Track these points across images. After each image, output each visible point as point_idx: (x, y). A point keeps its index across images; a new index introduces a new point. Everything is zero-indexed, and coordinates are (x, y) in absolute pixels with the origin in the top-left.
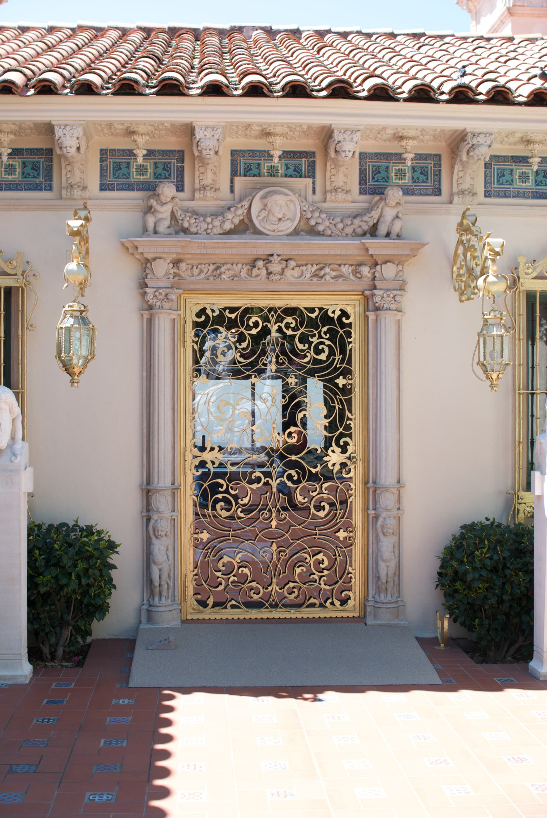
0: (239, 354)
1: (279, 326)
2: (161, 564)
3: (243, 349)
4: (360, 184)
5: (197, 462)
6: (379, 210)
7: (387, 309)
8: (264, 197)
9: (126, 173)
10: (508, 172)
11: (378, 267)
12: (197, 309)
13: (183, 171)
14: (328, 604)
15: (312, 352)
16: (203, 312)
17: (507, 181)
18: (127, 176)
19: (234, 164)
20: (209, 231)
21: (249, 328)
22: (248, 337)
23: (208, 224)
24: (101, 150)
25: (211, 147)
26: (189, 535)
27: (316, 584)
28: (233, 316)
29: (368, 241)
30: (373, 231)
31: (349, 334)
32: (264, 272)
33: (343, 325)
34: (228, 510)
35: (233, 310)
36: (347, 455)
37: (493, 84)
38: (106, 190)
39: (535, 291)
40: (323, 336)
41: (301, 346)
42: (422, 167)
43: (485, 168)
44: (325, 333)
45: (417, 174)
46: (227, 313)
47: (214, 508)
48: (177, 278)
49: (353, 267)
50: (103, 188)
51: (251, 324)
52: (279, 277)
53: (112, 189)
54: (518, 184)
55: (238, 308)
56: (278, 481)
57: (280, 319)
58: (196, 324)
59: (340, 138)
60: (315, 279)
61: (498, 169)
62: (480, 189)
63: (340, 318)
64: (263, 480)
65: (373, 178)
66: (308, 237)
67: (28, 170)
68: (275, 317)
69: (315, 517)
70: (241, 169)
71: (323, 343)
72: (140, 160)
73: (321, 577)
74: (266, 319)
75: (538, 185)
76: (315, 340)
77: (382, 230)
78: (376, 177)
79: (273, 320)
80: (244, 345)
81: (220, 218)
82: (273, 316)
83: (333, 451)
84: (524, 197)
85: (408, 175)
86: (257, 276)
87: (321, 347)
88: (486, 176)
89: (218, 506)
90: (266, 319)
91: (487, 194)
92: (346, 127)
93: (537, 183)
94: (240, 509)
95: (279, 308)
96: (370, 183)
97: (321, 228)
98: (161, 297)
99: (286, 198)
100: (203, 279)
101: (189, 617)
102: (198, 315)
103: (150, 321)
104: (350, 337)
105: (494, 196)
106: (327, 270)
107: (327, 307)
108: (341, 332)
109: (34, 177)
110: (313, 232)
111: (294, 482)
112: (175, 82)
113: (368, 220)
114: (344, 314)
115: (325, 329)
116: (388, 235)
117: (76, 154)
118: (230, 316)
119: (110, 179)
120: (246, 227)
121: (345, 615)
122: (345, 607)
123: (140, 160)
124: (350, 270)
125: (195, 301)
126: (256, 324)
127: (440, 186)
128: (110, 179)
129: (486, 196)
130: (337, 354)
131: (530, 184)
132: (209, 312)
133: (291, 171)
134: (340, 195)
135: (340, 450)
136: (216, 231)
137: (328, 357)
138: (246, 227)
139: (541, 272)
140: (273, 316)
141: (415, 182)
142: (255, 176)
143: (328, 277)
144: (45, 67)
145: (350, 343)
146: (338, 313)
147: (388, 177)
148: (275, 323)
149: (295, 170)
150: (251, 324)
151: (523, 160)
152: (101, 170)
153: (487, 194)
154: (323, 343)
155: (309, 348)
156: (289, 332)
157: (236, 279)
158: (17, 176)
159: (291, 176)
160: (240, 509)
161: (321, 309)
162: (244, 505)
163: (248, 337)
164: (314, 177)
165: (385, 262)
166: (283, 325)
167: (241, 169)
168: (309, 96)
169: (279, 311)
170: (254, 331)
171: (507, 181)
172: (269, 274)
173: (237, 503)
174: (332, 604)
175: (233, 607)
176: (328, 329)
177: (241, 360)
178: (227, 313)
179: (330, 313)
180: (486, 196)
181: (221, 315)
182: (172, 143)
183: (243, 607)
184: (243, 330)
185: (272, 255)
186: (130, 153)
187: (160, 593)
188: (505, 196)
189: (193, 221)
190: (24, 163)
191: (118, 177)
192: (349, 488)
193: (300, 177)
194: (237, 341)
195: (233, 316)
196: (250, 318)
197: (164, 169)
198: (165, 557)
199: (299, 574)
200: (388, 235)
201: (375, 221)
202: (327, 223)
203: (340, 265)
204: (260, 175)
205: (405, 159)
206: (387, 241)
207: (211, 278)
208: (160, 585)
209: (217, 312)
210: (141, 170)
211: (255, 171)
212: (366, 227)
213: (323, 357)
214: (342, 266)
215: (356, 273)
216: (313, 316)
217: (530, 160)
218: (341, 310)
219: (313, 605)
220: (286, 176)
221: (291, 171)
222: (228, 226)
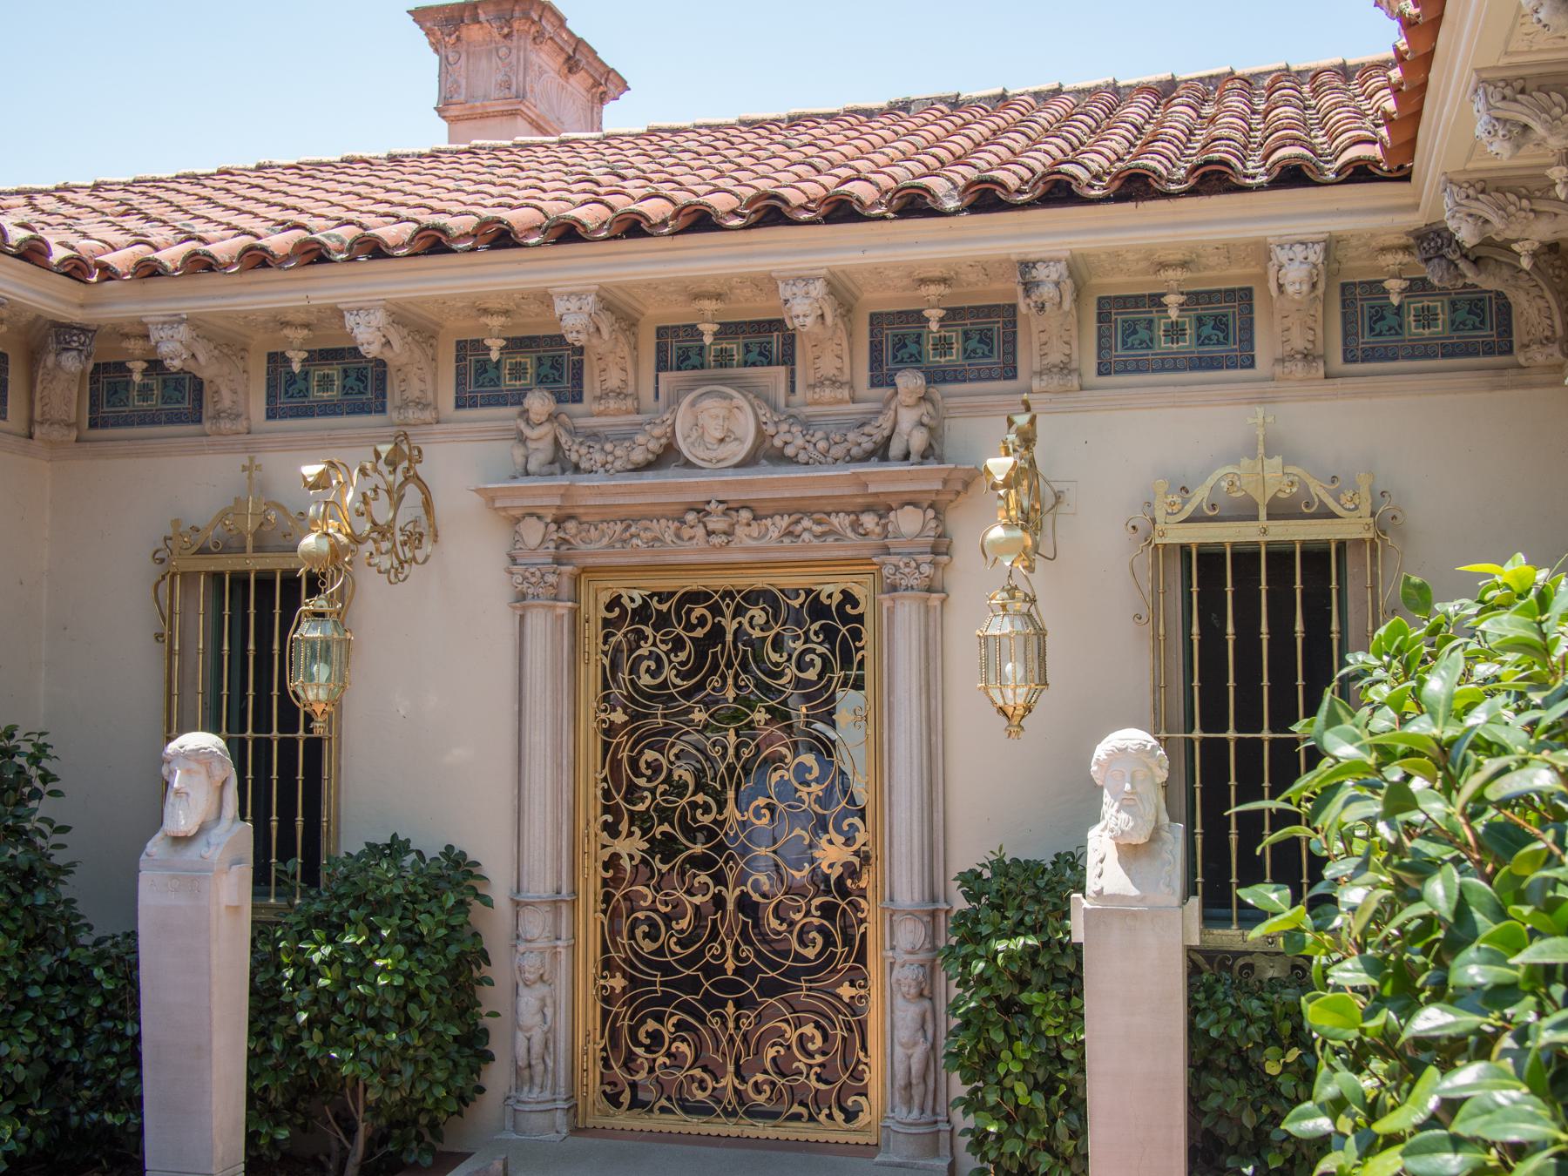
0: (674, 672)
1: (740, 623)
2: (530, 1029)
3: (682, 664)
4: (871, 370)
5: (605, 855)
6: (892, 413)
7: (906, 589)
8: (693, 404)
9: (1147, 338)
10: (1144, 324)
11: (892, 514)
12: (605, 598)
13: (581, 368)
14: (822, 1117)
15: (793, 667)
16: (615, 602)
17: (1142, 342)
18: (1149, 344)
19: (661, 350)
20: (608, 466)
21: (690, 627)
22: (689, 643)
23: (607, 454)
24: (458, 343)
25: (579, 327)
26: (873, 992)
27: (802, 1079)
28: (664, 607)
29: (873, 468)
30: (881, 452)
31: (857, 635)
32: (700, 531)
33: (846, 619)
34: (655, 939)
35: (663, 597)
36: (855, 847)
37: (307, 234)
38: (464, 406)
39: (1328, 542)
40: (814, 638)
41: (775, 657)
42: (1471, 301)
43: (1099, 321)
44: (816, 633)
45: (973, 344)
46: (654, 603)
47: (632, 936)
48: (564, 548)
49: (853, 517)
50: (271, 414)
51: (694, 621)
52: (724, 539)
53: (474, 405)
54: (1164, 345)
55: (673, 594)
56: (737, 892)
57: (739, 611)
58: (606, 623)
59: (788, 295)
60: (787, 540)
61: (1124, 321)
62: (1090, 363)
63: (840, 606)
64: (713, 890)
65: (895, 357)
66: (770, 467)
67: (351, 382)
68: (732, 607)
69: (799, 957)
70: (673, 356)
71: (813, 651)
72: (1173, 314)
73: (810, 1066)
74: (716, 610)
75: (1203, 344)
76: (799, 646)
77: (896, 448)
78: (1377, 327)
79: (728, 613)
80: (683, 656)
81: (627, 444)
82: (728, 606)
83: (830, 842)
84: (1175, 369)
85: (957, 346)
86: (691, 538)
87: (808, 658)
88: (1100, 337)
89: (639, 933)
90: (716, 610)
91: (1103, 371)
92: (795, 274)
93: (1201, 340)
94: (674, 939)
95: (739, 592)
96: (1488, 333)
97: (790, 451)
98: (533, 580)
99: (726, 403)
100: (608, 546)
101: (590, 1123)
102: (609, 608)
103: (522, 617)
104: (860, 640)
105: (1116, 372)
106: (806, 523)
107: (818, 588)
108: (844, 630)
109: (360, 393)
110: (780, 458)
111: (764, 896)
112: (773, 202)
113: (874, 431)
114: (848, 598)
115: (816, 626)
116: (906, 456)
117: (818, 329)
118: (659, 607)
119: (470, 389)
120: (667, 456)
121: (853, 1138)
122: (855, 1125)
123: (1173, 314)
124: (847, 522)
125: (604, 584)
126: (702, 621)
127: (1015, 361)
128: (470, 389)
129: (1100, 373)
130: (837, 666)
131: (1187, 344)
132: (625, 601)
133: (753, 356)
134: (828, 391)
135: (843, 839)
136: (618, 464)
137: (820, 676)
138: (667, 456)
139: (1199, 508)
140: (728, 606)
141: (969, 357)
142: (694, 368)
143: (806, 536)
144: (695, 188)
145: (858, 649)
146: (838, 598)
147: (920, 353)
148: (734, 618)
149: (761, 354)
150: (694, 621)
151: (1156, 300)
152: (458, 374)
153: (1103, 371)
154: (813, 651)
155: (789, 660)
156: (757, 633)
157: (657, 544)
158: (334, 393)
159: (754, 364)
160: (674, 939)
161: (808, 592)
162: (682, 931)
163: (689, 643)
164: (793, 364)
165: (902, 505)
166: (745, 621)
167: (673, 356)
168: (579, 239)
169: (738, 598)
170: (699, 633)
171: (1142, 342)
172: (709, 533)
173: (669, 927)
174: (830, 1116)
175: (663, 1110)
176: (822, 626)
177: (678, 681)
178: (654, 603)
179: (823, 598)
180: (1100, 373)
181: (645, 604)
182: (1233, 275)
183: (678, 1111)
184: (679, 630)
185: (709, 502)
186: (918, 317)
187: (531, 1078)
188: (1138, 370)
189: (583, 450)
190: (345, 371)
191: (482, 386)
192: (856, 908)
193: (770, 364)
194: (671, 650)
195: (664, 607)
196: (690, 611)
197: (552, 367)
198: (538, 1018)
199: (774, 1059)
200: (906, 456)
201: (886, 433)
202: (800, 441)
203: (829, 514)
204: (702, 366)
205: (928, 320)
206: (904, 467)
207: (618, 545)
208: (530, 1066)
209: (639, 601)
210: (1175, 331)
211: (695, 360)
212: (867, 445)
213: (812, 674)
214: (833, 516)
215: (855, 526)
216: (796, 603)
217: (1166, 300)
218: (843, 592)
219: (797, 1117)
220: (746, 364)
221: (753, 356)
222: (639, 456)
